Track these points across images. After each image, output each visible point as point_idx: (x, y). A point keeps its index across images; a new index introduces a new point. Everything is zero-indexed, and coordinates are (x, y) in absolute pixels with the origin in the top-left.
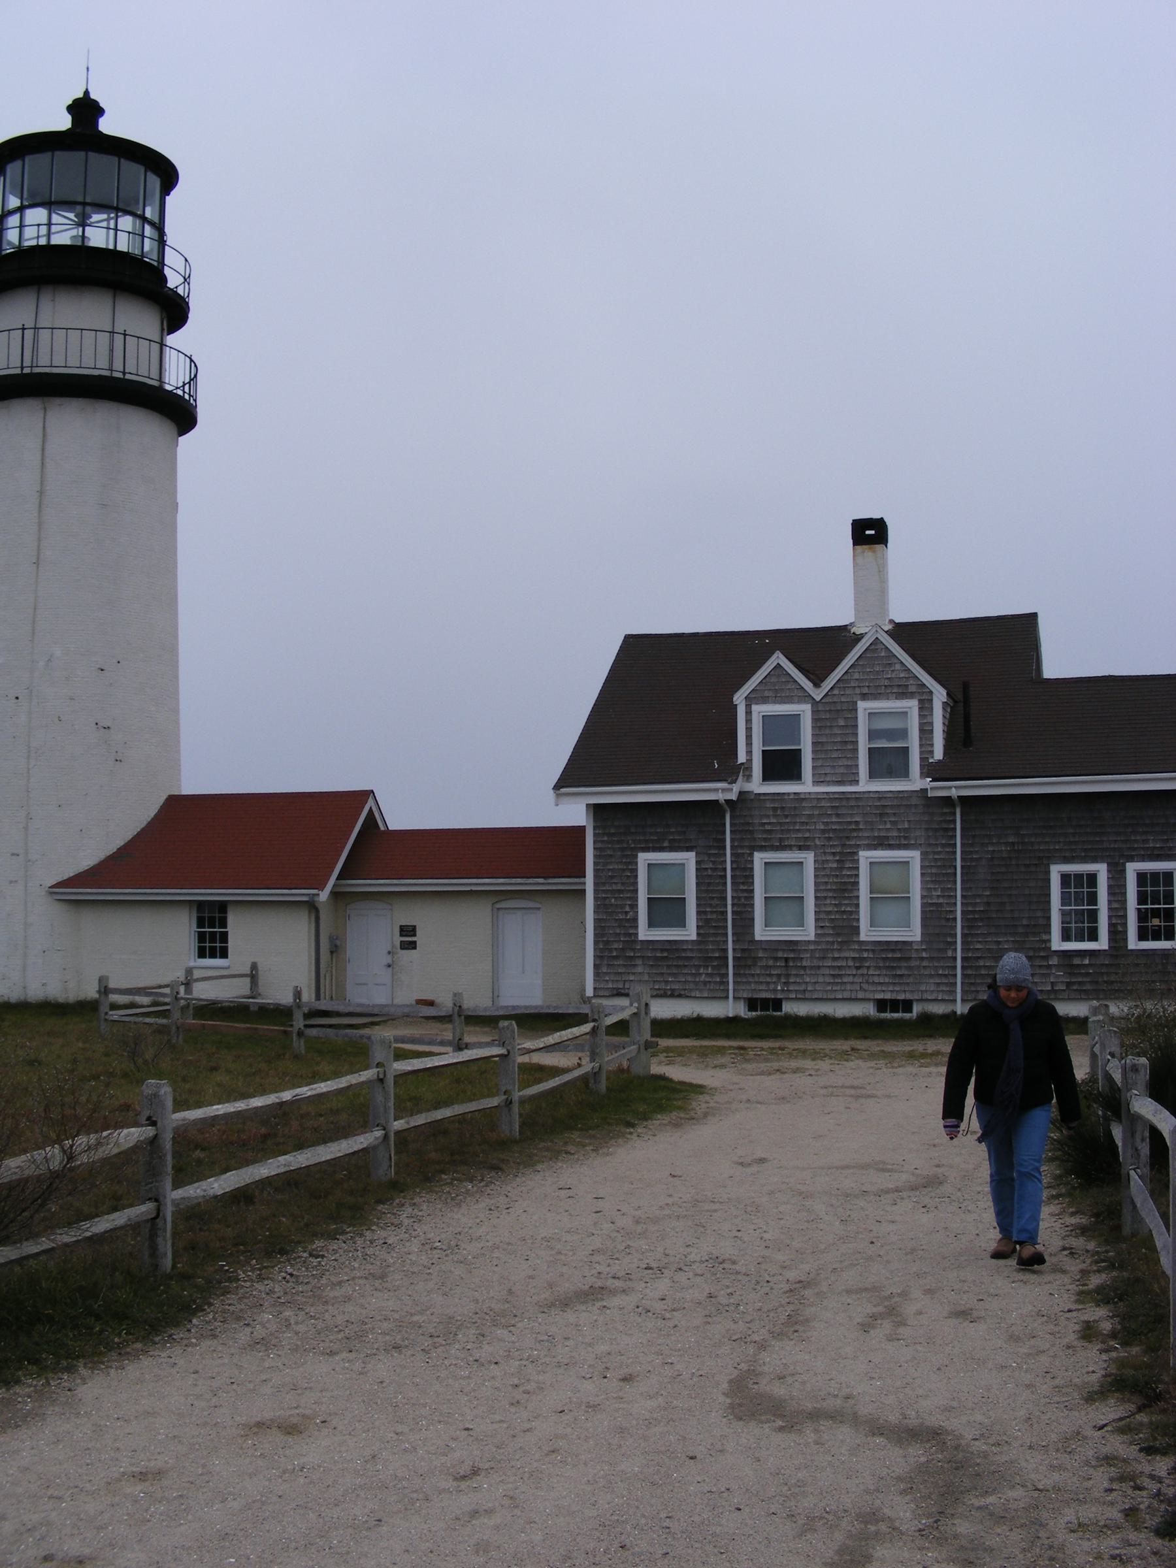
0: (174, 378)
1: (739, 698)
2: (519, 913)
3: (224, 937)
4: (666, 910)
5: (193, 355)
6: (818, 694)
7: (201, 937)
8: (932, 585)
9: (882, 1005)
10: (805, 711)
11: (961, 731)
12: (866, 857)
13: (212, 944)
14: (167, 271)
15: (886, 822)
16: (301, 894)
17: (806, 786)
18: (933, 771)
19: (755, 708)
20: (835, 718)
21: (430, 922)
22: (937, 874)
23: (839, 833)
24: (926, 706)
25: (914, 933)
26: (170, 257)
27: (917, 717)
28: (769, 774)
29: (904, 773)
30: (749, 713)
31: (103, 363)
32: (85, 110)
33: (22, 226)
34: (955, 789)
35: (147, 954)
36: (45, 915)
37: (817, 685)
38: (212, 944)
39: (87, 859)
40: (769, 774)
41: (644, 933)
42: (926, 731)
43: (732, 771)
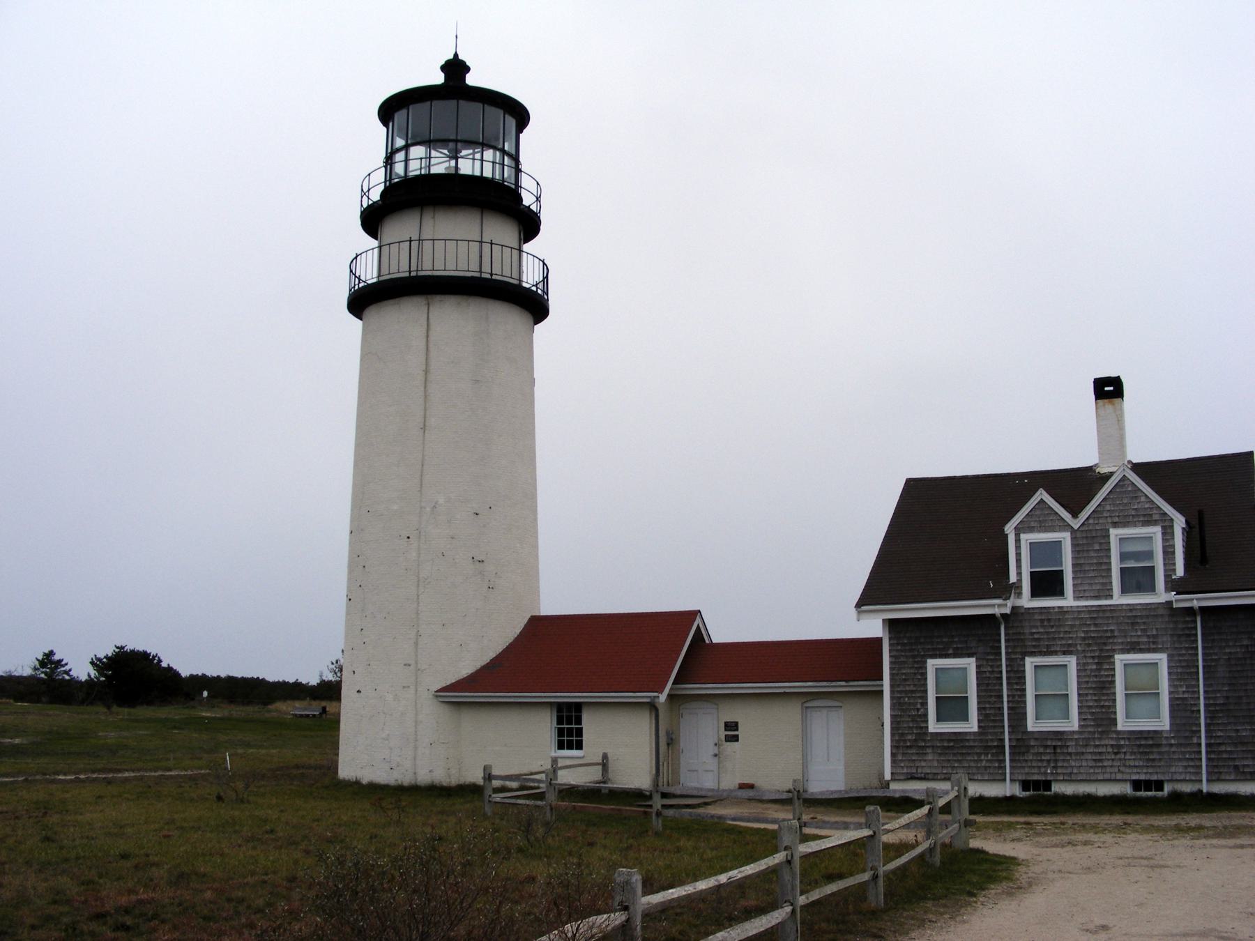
0: (530, 278)
1: (1009, 529)
2: (825, 711)
3: (580, 732)
4: (952, 707)
5: (545, 258)
6: (1076, 524)
7: (560, 732)
9: (1137, 785)
10: (1065, 538)
12: (1120, 659)
13: (570, 737)
14: (524, 194)
15: (1138, 629)
16: (643, 697)
17: (1068, 600)
18: (1175, 585)
19: (1023, 536)
20: (1091, 544)
21: (750, 718)
22: (1182, 673)
23: (1098, 640)
24: (1168, 532)
25: (1164, 723)
26: (525, 181)
27: (1161, 541)
28: (1035, 593)
29: (1152, 588)
30: (1018, 541)
31: (474, 266)
32: (455, 68)
33: (407, 160)
34: (1197, 601)
35: (517, 746)
36: (432, 715)
37: (1075, 515)
38: (570, 737)
39: (467, 666)
40: (1035, 593)
41: (933, 726)
42: (1169, 553)
43: (1006, 589)
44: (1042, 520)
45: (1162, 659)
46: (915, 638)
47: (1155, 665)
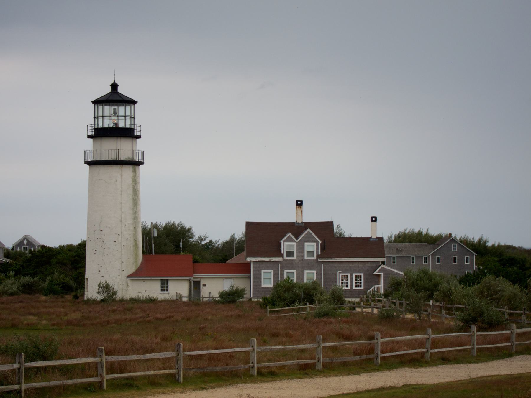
1: (282, 242)
3: (167, 287)
7: (162, 287)
8: (311, 215)
11: (323, 248)
13: (165, 288)
16: (188, 278)
19: (285, 243)
28: (287, 256)
38: (165, 288)
40: (287, 256)
43: (281, 255)
44: (289, 240)
45: (315, 272)
47: (313, 273)
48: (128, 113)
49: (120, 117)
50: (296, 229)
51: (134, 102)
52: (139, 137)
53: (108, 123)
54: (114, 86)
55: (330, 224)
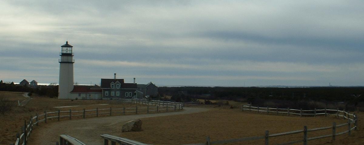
4: (107, 94)
8: (118, 77)
15: (118, 90)
20: (115, 85)
27: (120, 85)
37: (115, 83)
38: (80, 96)
39: (71, 91)
43: (111, 87)
46: (105, 90)
48: (71, 50)
49: (68, 51)
50: (115, 80)
51: (72, 47)
52: (73, 56)
53: (65, 52)
54: (67, 42)
55: (123, 79)
